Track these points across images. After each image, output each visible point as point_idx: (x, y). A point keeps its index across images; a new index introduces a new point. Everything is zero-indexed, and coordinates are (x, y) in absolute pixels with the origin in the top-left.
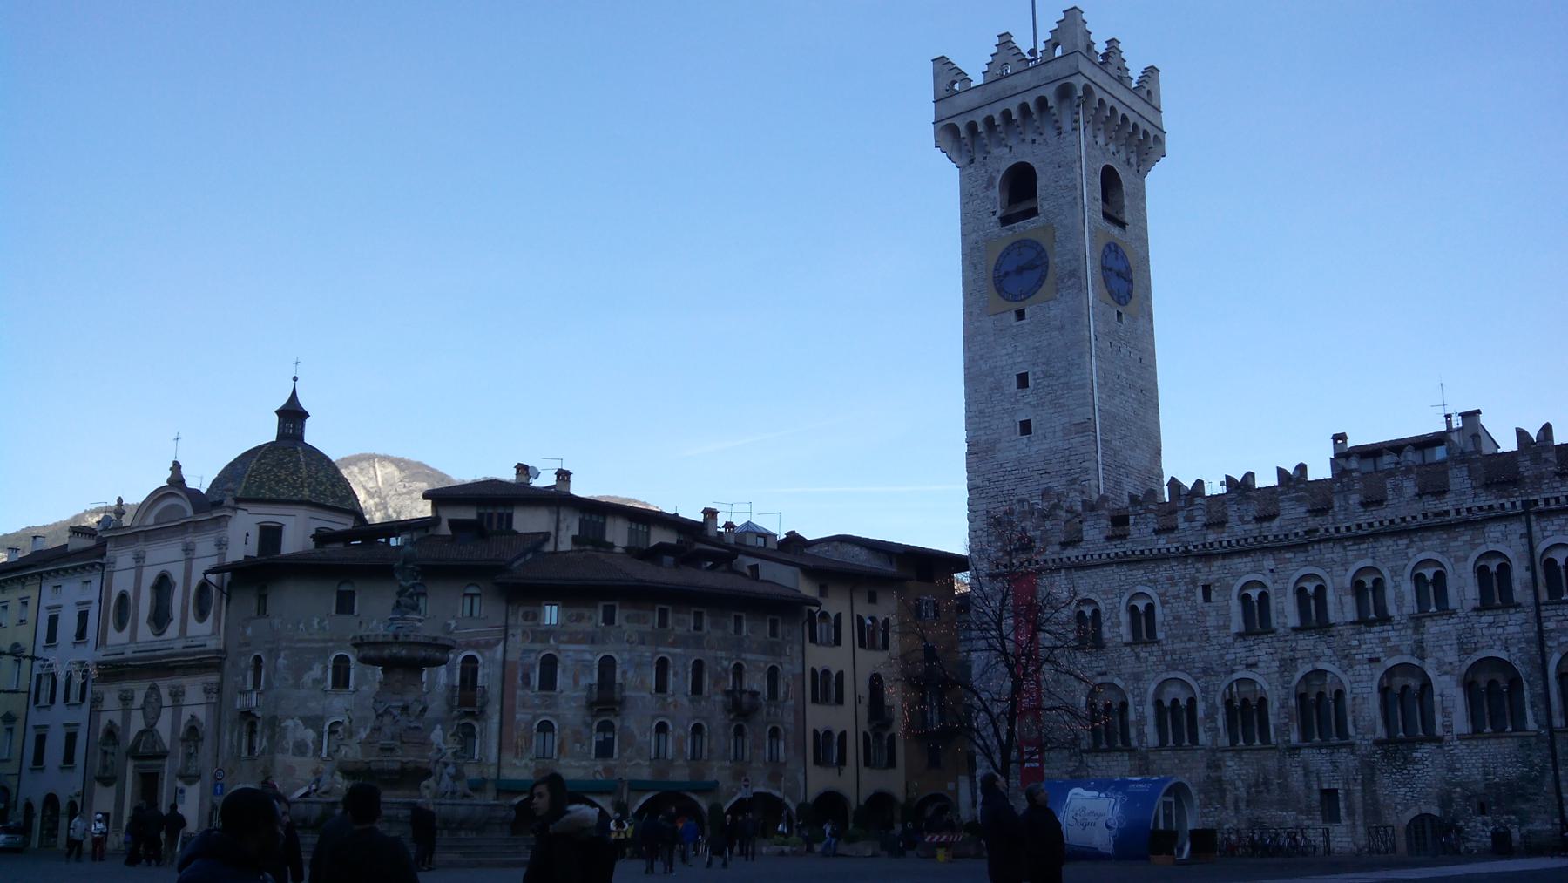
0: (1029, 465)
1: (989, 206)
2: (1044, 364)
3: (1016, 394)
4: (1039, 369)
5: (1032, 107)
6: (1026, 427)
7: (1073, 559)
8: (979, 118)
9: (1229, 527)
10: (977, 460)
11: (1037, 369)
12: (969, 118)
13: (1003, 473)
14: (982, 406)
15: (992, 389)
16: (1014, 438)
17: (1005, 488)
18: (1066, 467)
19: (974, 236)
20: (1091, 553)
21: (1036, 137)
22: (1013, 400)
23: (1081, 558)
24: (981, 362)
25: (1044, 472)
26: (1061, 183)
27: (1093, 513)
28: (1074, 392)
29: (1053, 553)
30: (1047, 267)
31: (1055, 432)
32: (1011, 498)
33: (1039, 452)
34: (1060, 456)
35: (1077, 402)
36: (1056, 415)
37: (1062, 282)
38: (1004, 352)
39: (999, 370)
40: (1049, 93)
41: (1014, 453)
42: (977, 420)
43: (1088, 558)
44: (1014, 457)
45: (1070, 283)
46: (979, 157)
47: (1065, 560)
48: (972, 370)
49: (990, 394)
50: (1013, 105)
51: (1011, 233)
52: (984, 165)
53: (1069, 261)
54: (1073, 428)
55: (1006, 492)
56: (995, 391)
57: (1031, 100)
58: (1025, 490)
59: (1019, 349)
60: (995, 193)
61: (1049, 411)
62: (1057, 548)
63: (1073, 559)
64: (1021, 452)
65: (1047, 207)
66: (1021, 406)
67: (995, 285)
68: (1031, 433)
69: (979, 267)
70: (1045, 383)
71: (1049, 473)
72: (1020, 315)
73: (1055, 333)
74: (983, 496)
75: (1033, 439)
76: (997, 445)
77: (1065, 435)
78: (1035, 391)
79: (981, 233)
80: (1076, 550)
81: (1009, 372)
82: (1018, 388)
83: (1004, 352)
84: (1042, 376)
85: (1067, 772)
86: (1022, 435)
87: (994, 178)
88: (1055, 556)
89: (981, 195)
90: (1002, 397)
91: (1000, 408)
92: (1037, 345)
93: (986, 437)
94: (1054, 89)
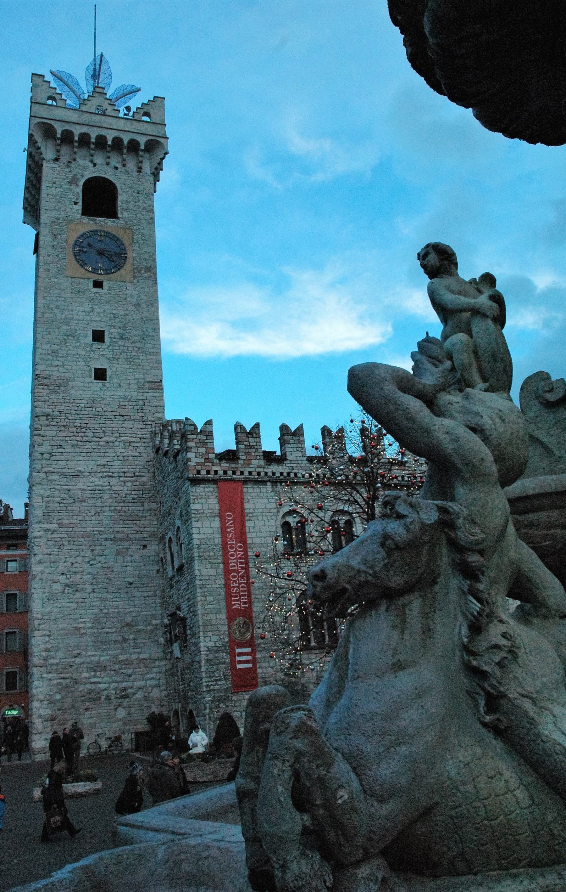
0: (103, 406)
1: (72, 197)
2: (119, 328)
3: (92, 345)
4: (116, 331)
5: (126, 142)
6: (100, 374)
7: (278, 474)
8: (77, 131)
9: (408, 467)
10: (48, 391)
11: (112, 330)
12: (67, 127)
13: (76, 408)
14: (55, 347)
15: (67, 336)
16: (88, 380)
17: (77, 421)
18: (140, 414)
19: (54, 213)
20: (294, 471)
21: (119, 166)
22: (88, 349)
23: (285, 474)
24: (56, 311)
25: (118, 414)
26: (140, 204)
27: (294, 438)
28: (148, 356)
29: (258, 467)
30: (126, 257)
31: (130, 384)
32: (83, 430)
33: (114, 397)
34: (134, 404)
35: (151, 365)
36: (130, 370)
37: (139, 272)
38: (81, 309)
39: (77, 322)
40: (142, 140)
41: (88, 394)
42: (50, 357)
43: (292, 475)
44: (88, 396)
45: (146, 275)
46: (64, 159)
47: (270, 474)
48: (46, 315)
49: (65, 340)
50: (110, 137)
51: (92, 222)
52: (68, 167)
53: (145, 259)
54: (147, 385)
55: (79, 425)
56: (70, 337)
57: (126, 139)
58: (98, 426)
59: (96, 310)
60: (79, 190)
61: (124, 366)
62: (262, 462)
63: (278, 474)
64: (95, 393)
65: (127, 216)
66: (97, 356)
67: (75, 256)
68: (105, 379)
69: (59, 237)
70: (120, 343)
71: (123, 416)
72: (98, 284)
73: (131, 308)
74: (52, 423)
75: (108, 385)
76: (69, 383)
77: (139, 388)
78: (111, 348)
79: (63, 213)
80: (280, 467)
81: (85, 326)
82: (93, 341)
83: (81, 309)
84: (118, 337)
85: (282, 670)
86: (95, 379)
87: (78, 179)
88: (258, 470)
89: (64, 186)
90: (78, 344)
91: (75, 353)
92: (114, 312)
93: (58, 374)
94: (146, 139)
